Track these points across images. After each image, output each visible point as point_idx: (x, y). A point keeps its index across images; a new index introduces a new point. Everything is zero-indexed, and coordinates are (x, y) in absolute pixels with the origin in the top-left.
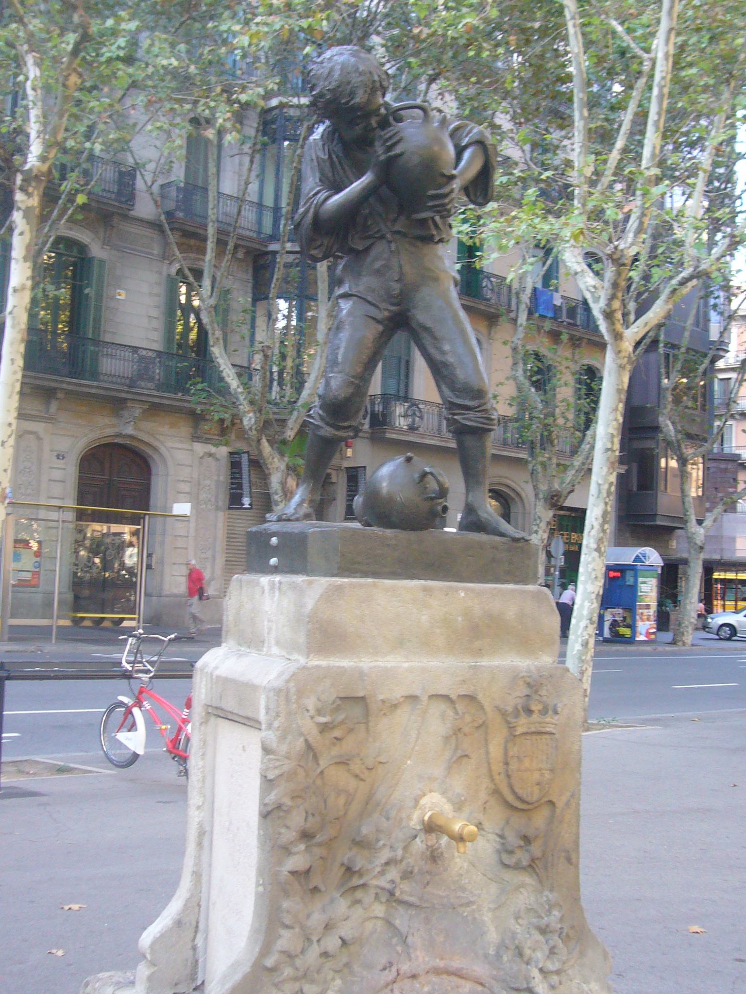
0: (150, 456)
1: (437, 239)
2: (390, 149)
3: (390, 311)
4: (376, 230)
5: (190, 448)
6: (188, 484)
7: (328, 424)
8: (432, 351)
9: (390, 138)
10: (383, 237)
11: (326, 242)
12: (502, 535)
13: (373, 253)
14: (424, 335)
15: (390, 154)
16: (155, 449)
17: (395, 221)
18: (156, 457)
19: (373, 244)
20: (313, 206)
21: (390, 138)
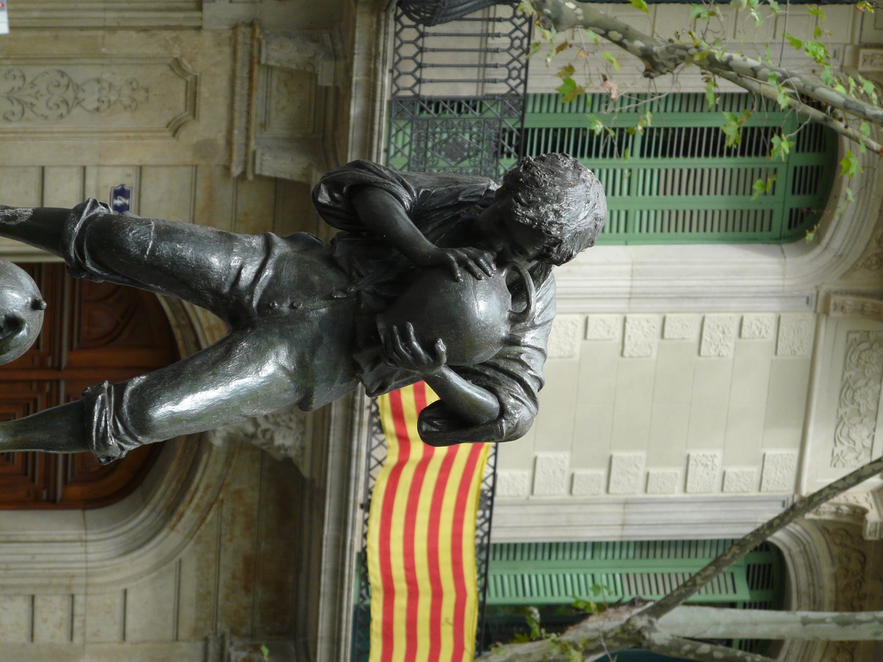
0: (144, 503)
1: (357, 357)
2: (463, 263)
3: (251, 301)
4: (362, 272)
5: (184, 633)
6: (61, 636)
7: (84, 225)
9: (479, 265)
11: (339, 206)
13: (331, 275)
14: (221, 350)
15: (456, 265)
16: (171, 511)
18: (143, 518)
20: (387, 181)
21: (479, 265)
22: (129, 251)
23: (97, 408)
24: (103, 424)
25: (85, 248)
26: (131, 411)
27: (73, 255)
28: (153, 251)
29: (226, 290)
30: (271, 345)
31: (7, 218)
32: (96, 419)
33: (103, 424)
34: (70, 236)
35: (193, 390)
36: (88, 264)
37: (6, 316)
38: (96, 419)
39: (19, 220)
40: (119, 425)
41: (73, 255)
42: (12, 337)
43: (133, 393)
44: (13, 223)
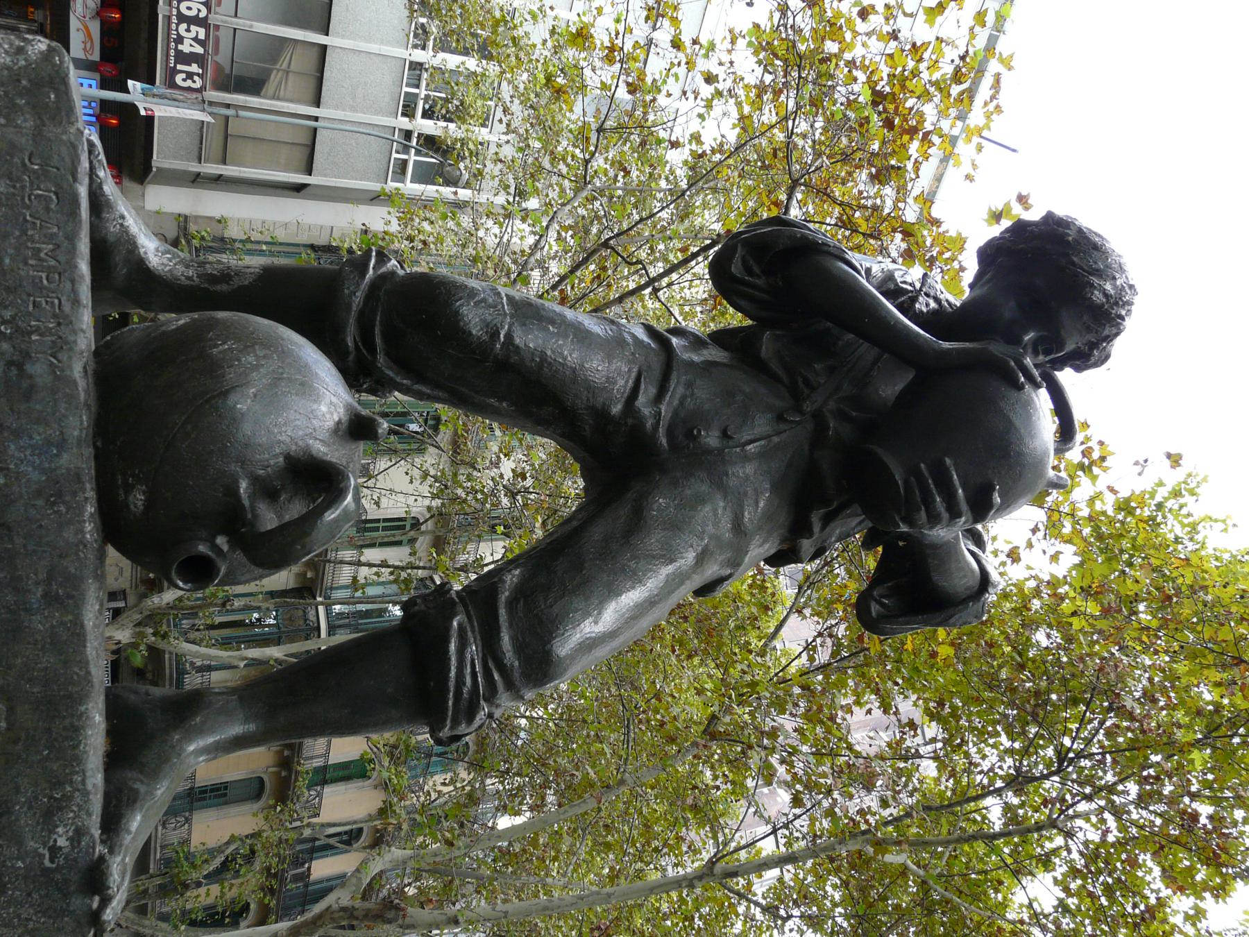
3: (656, 427)
8: (597, 532)
10: (797, 397)
12: (112, 824)
17: (841, 415)
19: (776, 378)
22: (470, 333)
23: (453, 647)
24: (468, 680)
25: (377, 330)
26: (519, 648)
27: (350, 343)
28: (509, 336)
29: (616, 409)
30: (700, 500)
31: (212, 279)
32: (453, 673)
33: (468, 680)
34: (349, 306)
35: (613, 592)
36: (381, 359)
37: (288, 457)
38: (453, 673)
39: (236, 282)
40: (496, 676)
41: (350, 343)
42: (318, 513)
43: (511, 603)
44: (223, 288)
